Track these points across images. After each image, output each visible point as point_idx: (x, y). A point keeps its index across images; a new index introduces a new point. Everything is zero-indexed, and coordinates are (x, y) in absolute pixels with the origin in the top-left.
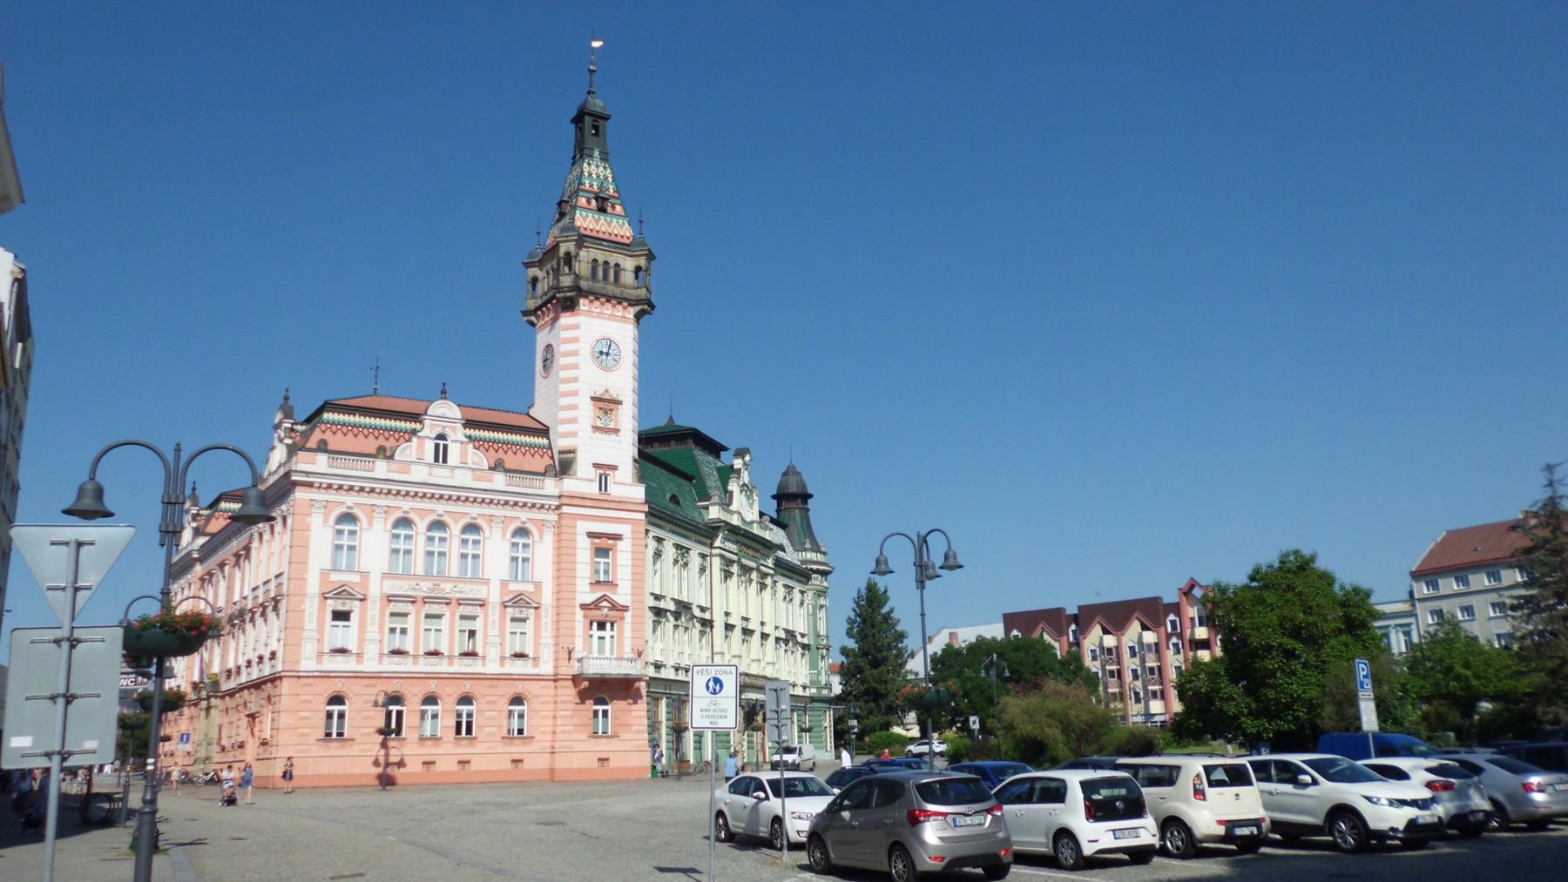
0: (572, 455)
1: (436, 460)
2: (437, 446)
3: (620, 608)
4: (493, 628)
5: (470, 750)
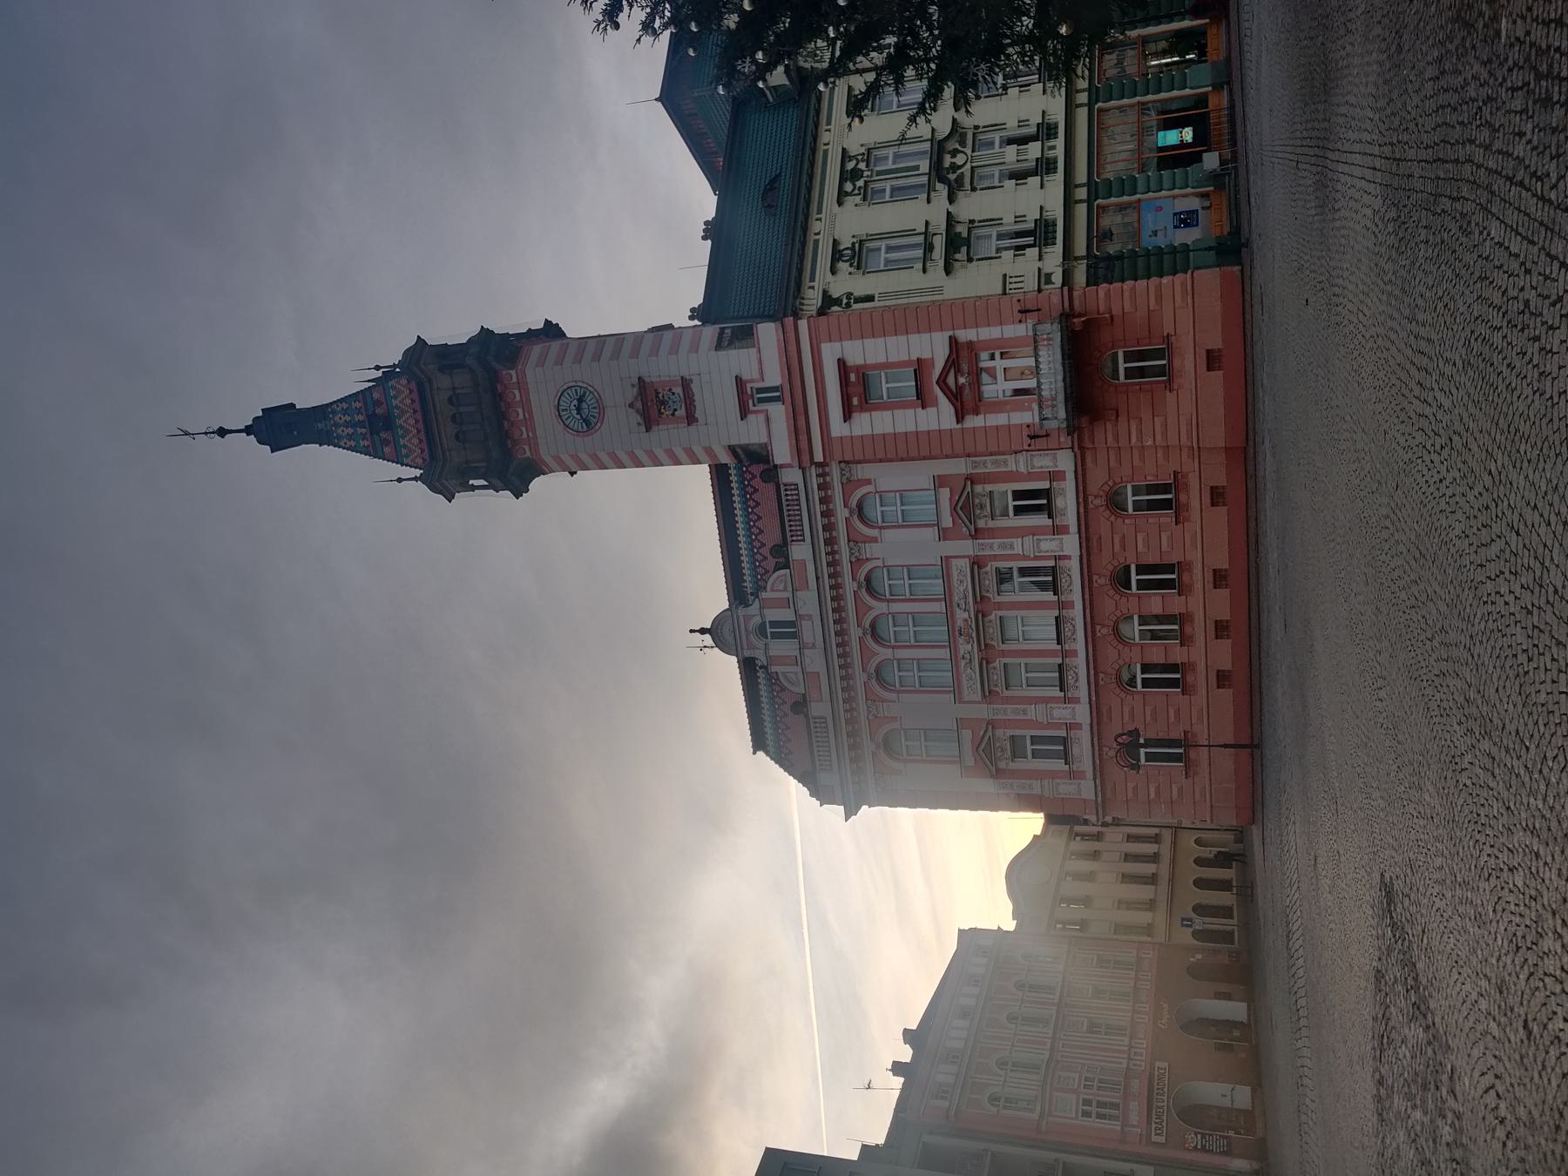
0: (739, 450)
1: (793, 636)
2: (775, 636)
3: (955, 356)
4: (1012, 547)
5: (1197, 570)
